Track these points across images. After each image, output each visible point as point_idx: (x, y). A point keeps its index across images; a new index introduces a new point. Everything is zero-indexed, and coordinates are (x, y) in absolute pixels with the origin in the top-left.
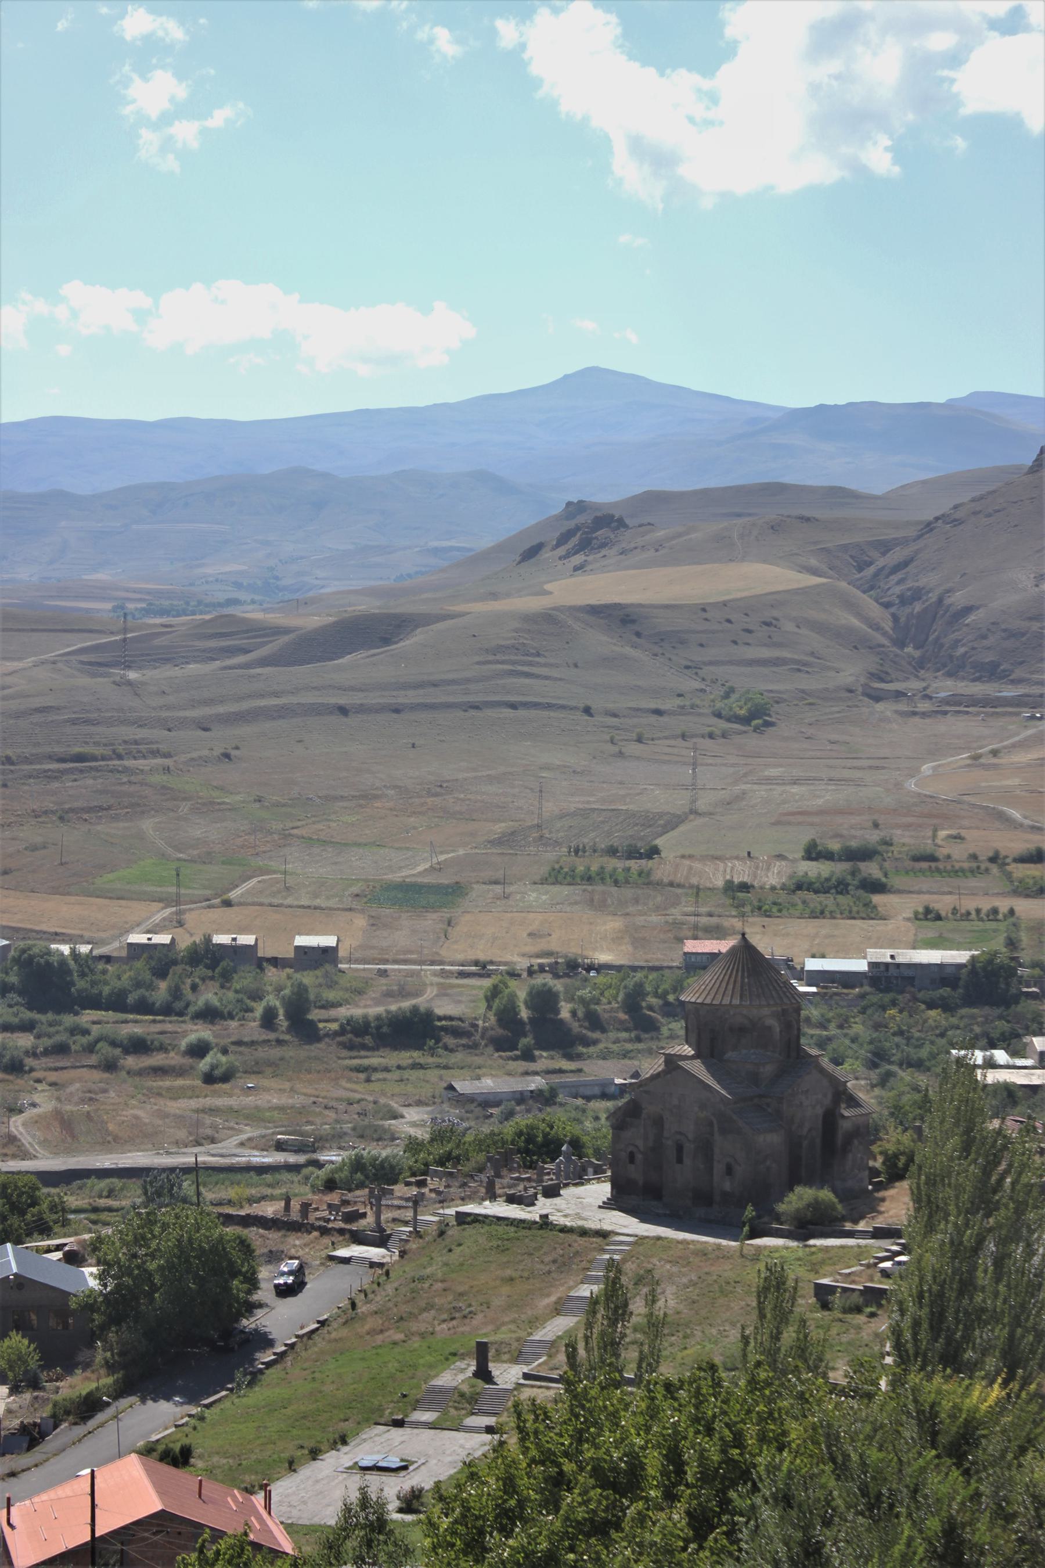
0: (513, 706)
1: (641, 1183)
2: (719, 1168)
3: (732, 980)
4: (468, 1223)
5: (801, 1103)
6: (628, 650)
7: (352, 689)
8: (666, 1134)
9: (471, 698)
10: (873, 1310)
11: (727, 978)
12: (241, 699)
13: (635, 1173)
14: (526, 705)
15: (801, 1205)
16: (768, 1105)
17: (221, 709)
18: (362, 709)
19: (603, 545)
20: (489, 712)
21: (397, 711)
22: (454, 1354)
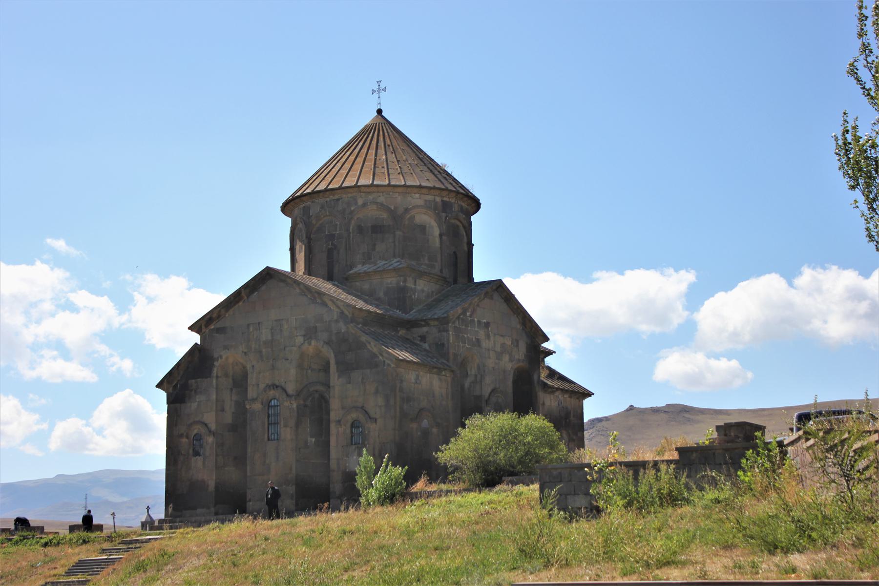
1: (212, 485)
3: (360, 160)
5: (478, 340)
8: (251, 393)
11: (352, 158)
13: (203, 471)
16: (423, 338)
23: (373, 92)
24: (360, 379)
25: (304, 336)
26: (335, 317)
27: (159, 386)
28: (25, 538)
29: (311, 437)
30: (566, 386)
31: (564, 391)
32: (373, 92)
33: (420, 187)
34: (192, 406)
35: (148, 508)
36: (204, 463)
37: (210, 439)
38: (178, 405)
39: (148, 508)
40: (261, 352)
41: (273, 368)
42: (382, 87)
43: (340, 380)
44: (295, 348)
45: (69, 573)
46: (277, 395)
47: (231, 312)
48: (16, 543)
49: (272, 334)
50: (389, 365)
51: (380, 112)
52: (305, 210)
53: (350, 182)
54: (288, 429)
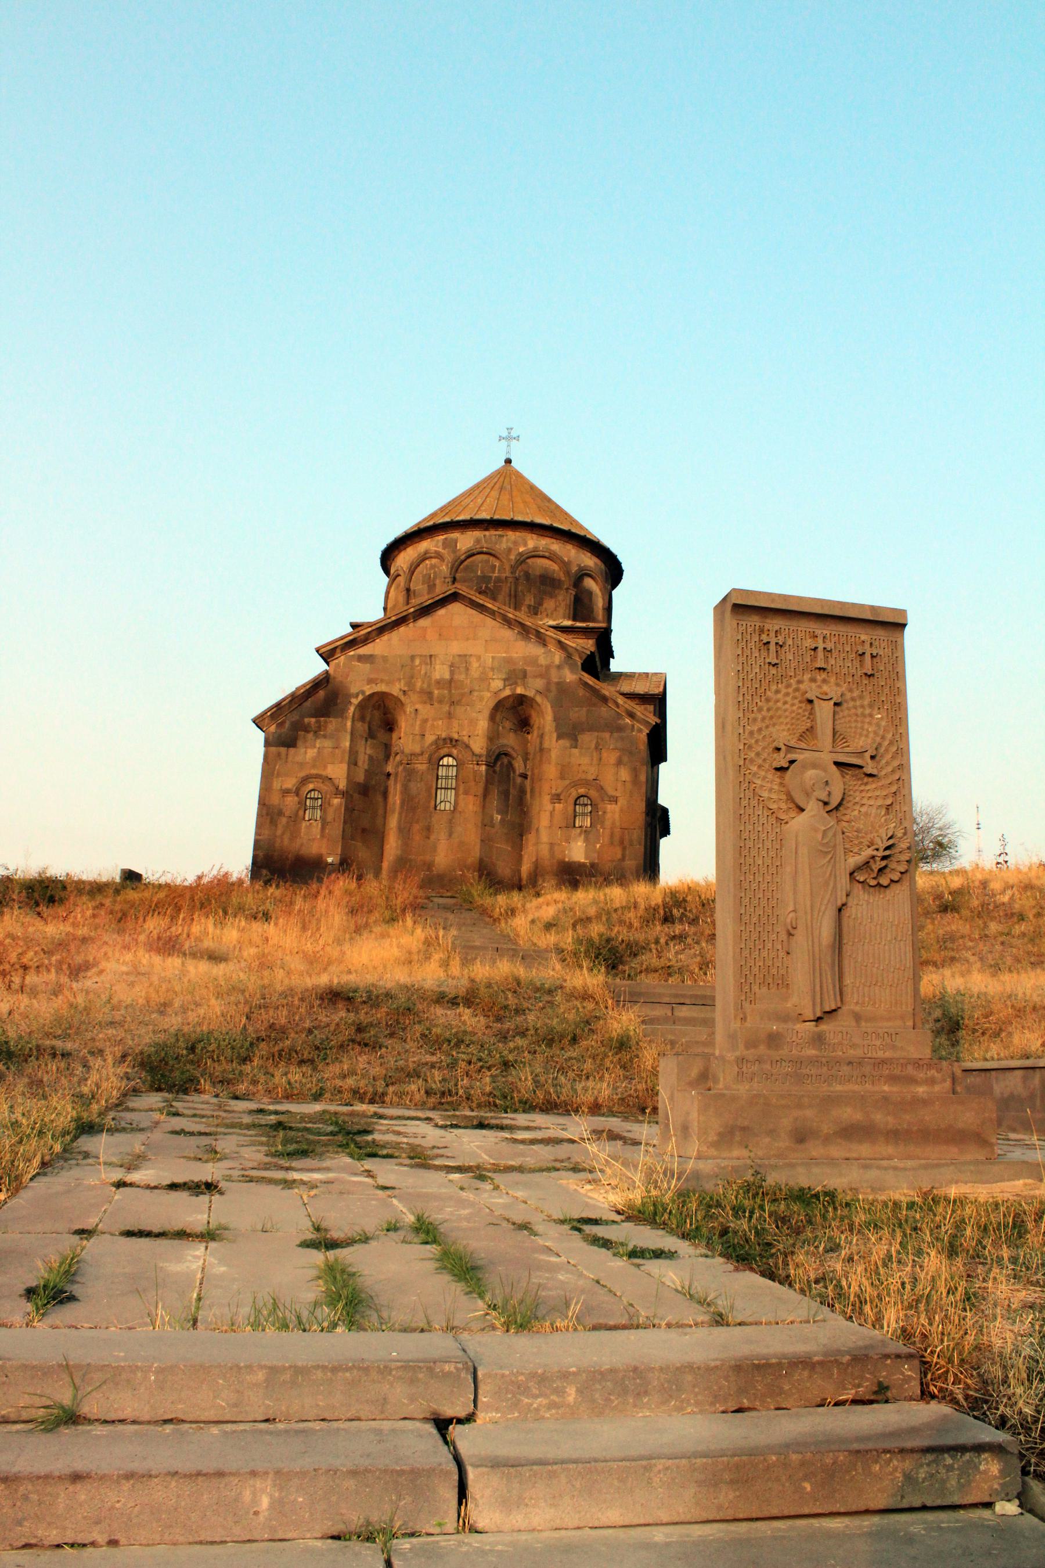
2: (546, 815)
23: (501, 438)
24: (593, 746)
25: (505, 680)
26: (557, 661)
29: (498, 813)
34: (307, 753)
36: (323, 828)
37: (336, 801)
38: (283, 750)
40: (430, 694)
41: (450, 716)
43: (561, 742)
44: (489, 695)
46: (455, 752)
47: (385, 637)
49: (452, 673)
50: (640, 731)
51: (508, 461)
54: (471, 798)
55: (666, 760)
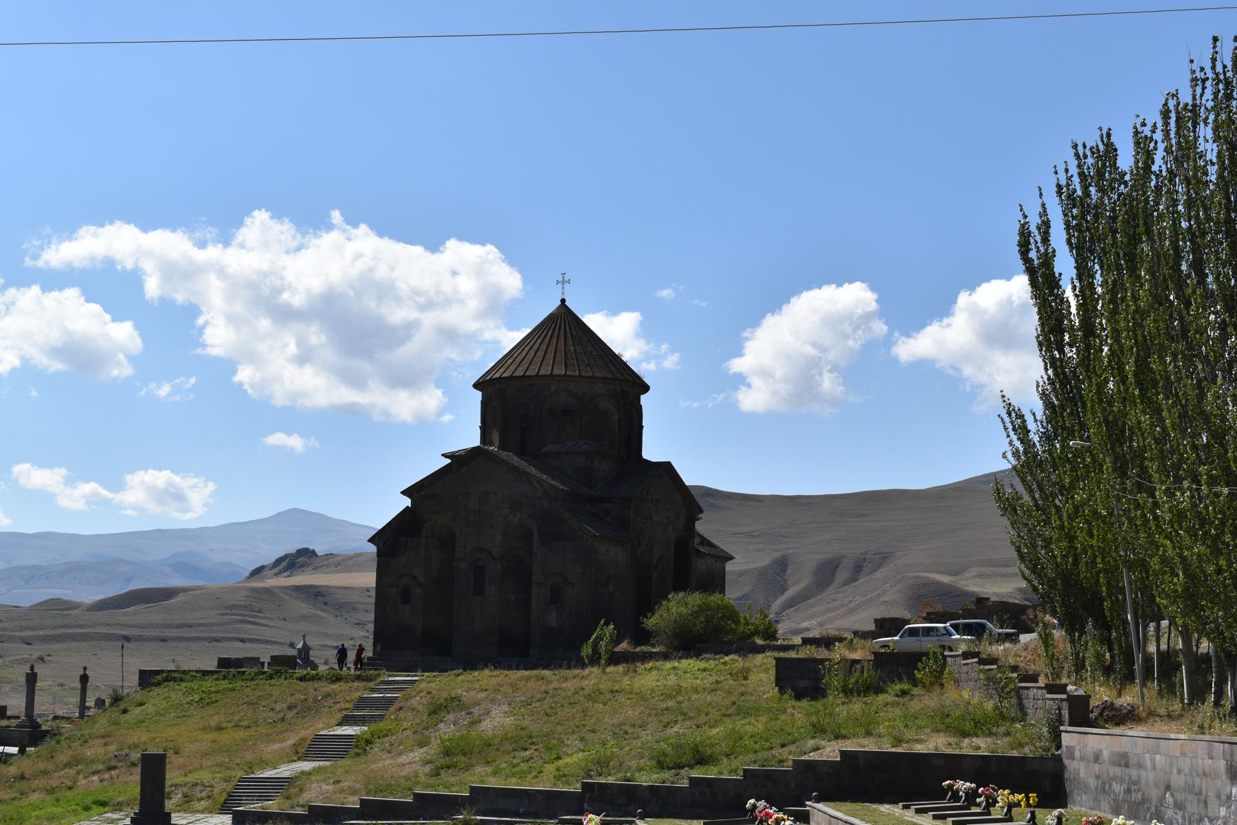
0: (243, 641)
3: (552, 349)
4: (158, 684)
6: (319, 612)
7: (134, 626)
9: (214, 635)
10: (906, 687)
11: (544, 347)
12: (56, 628)
14: (251, 641)
15: (683, 610)
17: (41, 633)
18: (139, 638)
19: (302, 566)
20: (227, 644)
21: (164, 640)
22: (104, 804)
27: (371, 540)
28: (277, 672)
30: (713, 551)
31: (712, 556)
32: (558, 282)
33: (605, 378)
35: (304, 636)
37: (418, 591)
39: (304, 636)
42: (566, 278)
45: (357, 708)
48: (271, 677)
51: (563, 301)
52: (501, 392)
53: (545, 371)
55: (701, 511)
